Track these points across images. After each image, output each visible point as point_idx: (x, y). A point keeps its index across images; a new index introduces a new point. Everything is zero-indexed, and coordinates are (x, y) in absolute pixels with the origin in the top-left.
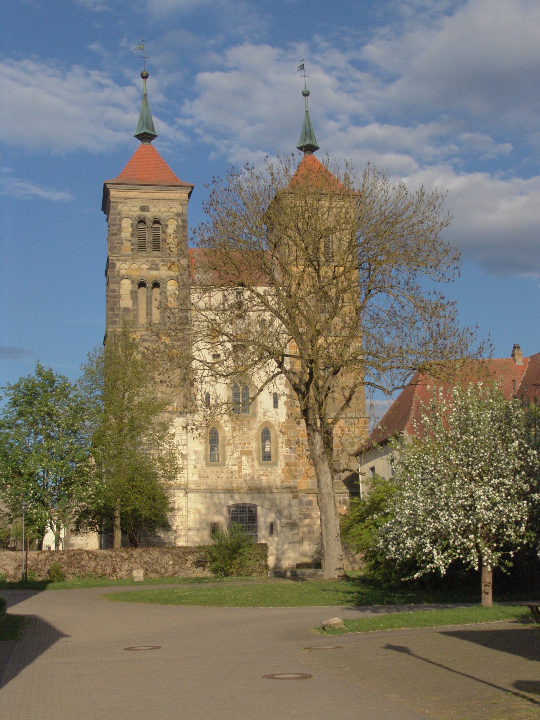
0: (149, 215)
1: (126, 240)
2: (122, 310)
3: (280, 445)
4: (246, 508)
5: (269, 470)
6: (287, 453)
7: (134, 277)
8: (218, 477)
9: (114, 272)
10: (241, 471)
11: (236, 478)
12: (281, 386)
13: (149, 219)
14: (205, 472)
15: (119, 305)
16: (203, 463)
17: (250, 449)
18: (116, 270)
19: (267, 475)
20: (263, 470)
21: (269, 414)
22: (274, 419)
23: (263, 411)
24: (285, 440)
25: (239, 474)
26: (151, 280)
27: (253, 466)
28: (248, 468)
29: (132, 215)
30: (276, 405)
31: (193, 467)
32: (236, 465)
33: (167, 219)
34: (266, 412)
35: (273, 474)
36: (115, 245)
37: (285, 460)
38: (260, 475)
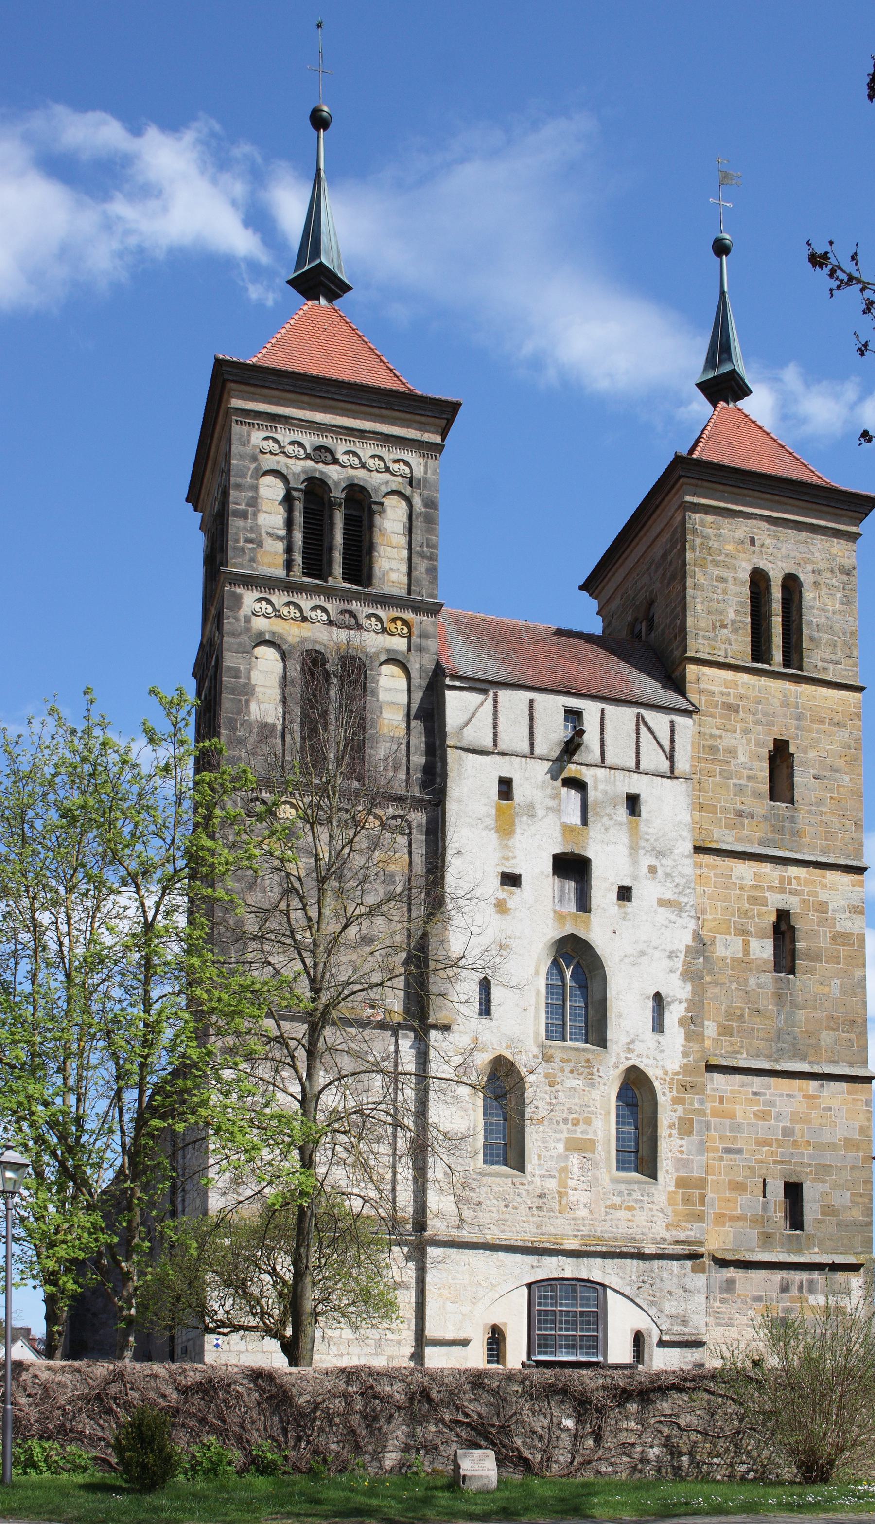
3: (663, 1131)
5: (637, 1195)
6: (682, 1152)
7: (290, 639)
8: (506, 1206)
10: (567, 1194)
11: (551, 1210)
12: (672, 975)
17: (590, 1136)
19: (630, 1209)
20: (620, 1193)
21: (639, 1047)
22: (651, 1062)
23: (624, 1039)
24: (679, 1119)
30: (658, 1026)
34: (632, 1041)
37: (677, 1170)
38: (613, 1207)
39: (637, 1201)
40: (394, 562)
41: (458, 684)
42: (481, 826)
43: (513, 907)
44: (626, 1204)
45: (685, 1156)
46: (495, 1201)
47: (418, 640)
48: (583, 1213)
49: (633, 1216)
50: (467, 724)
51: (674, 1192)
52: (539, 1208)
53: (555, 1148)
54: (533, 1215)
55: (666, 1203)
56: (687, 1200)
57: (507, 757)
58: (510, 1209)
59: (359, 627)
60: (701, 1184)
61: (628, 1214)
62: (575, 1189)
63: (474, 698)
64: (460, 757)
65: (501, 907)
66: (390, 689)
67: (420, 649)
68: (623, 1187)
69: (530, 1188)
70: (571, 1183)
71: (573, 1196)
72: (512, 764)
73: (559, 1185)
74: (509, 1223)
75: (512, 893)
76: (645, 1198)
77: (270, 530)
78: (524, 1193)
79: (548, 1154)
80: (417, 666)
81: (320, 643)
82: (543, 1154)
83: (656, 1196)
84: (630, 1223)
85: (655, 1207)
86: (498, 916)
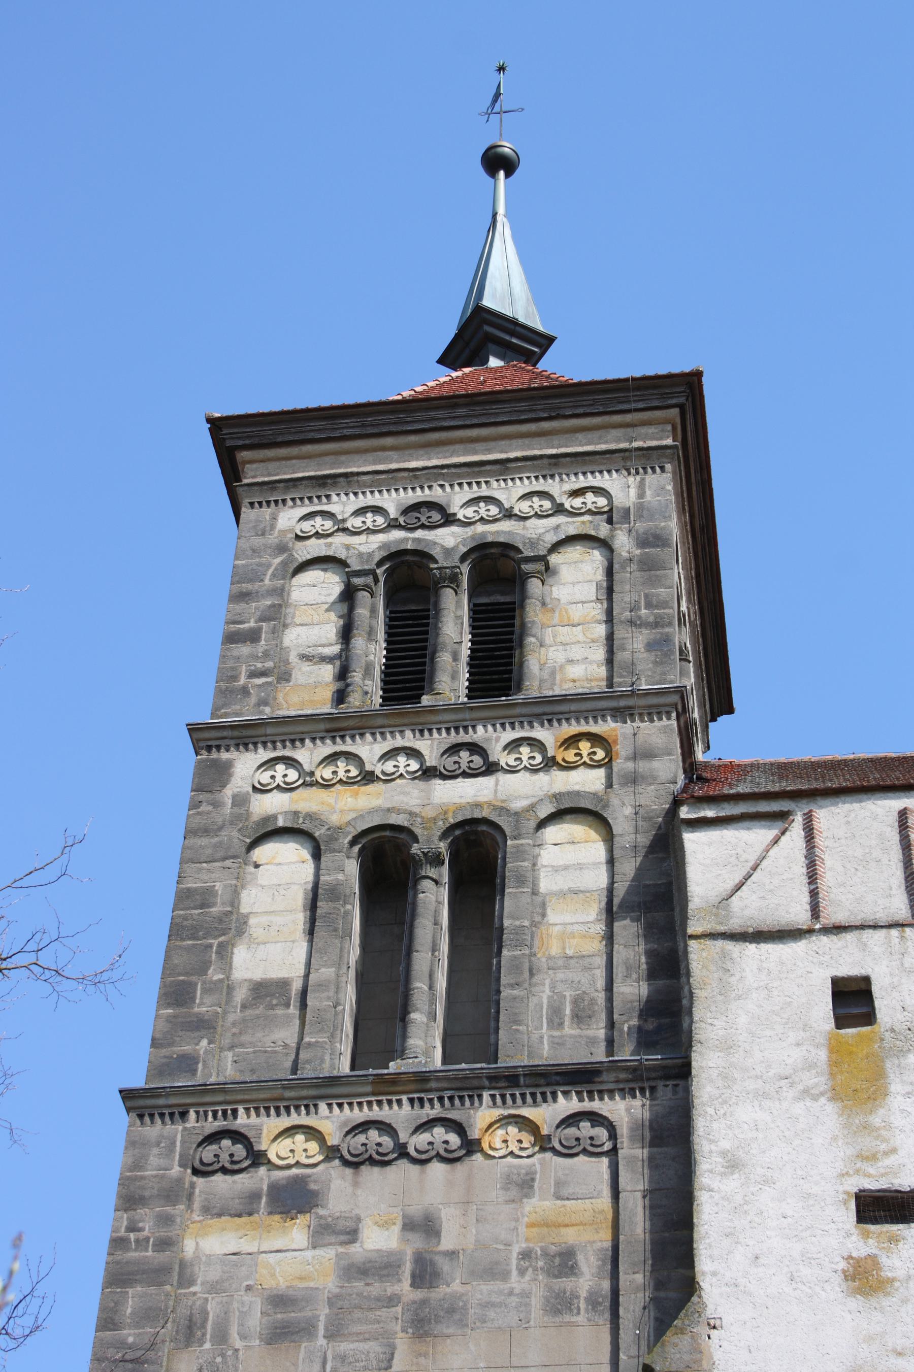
0: (447, 540)
1: (305, 657)
2: (240, 995)
7: (335, 819)
9: (216, 804)
13: (448, 552)
15: (227, 967)
18: (228, 792)
26: (442, 825)
29: (348, 547)
33: (551, 538)
36: (242, 680)
40: (576, 648)
41: (710, 813)
42: (790, 1094)
43: (900, 1273)
47: (630, 765)
50: (739, 887)
57: (849, 937)
59: (491, 768)
63: (756, 837)
64: (724, 955)
65: (863, 1278)
66: (566, 868)
67: (633, 780)
72: (864, 947)
75: (894, 1240)
77: (307, 651)
80: (628, 811)
81: (399, 811)
86: (854, 1303)
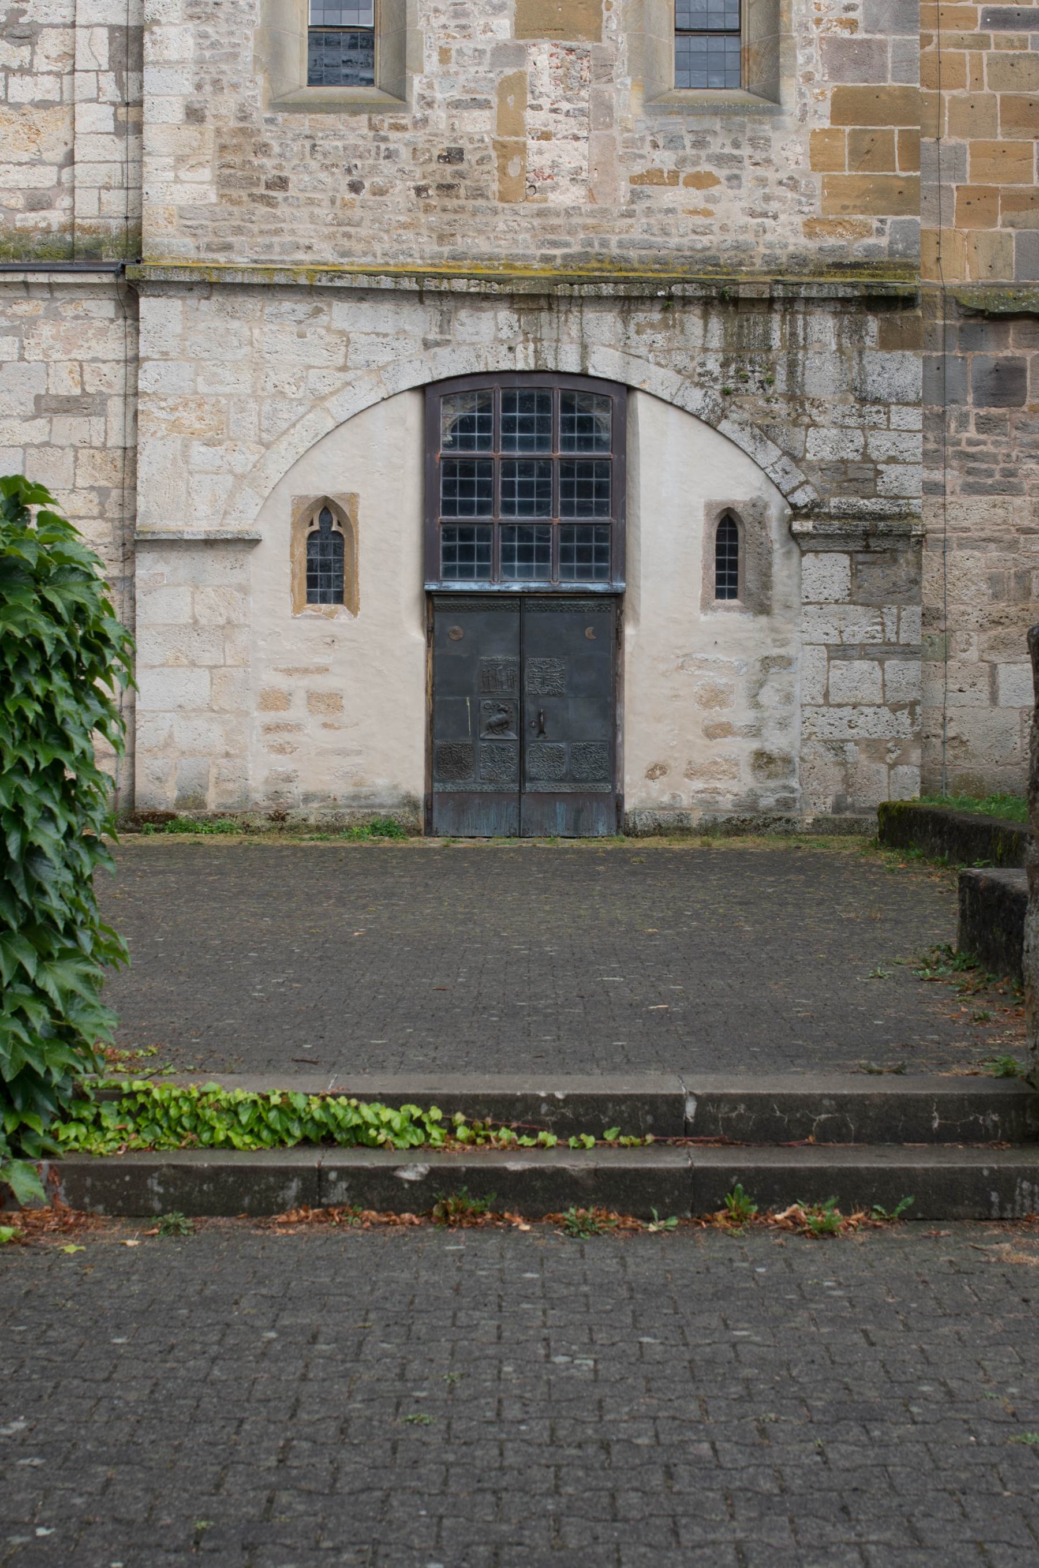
4: (544, 404)
6: (852, 25)
8: (355, 187)
10: (522, 150)
11: (479, 193)
14: (263, 149)
16: (255, 90)
19: (699, 181)
20: (673, 142)
25: (502, 170)
27: (603, 111)
28: (568, 126)
31: (180, 115)
32: (485, 105)
35: (749, 173)
37: (836, 72)
38: (653, 177)
39: (720, 160)
44: (690, 170)
45: (860, 35)
46: (323, 176)
48: (567, 196)
49: (711, 199)
51: (825, 132)
52: (447, 188)
53: (487, 29)
54: (428, 209)
55: (806, 164)
56: (864, 154)
58: (365, 194)
60: (907, 108)
61: (695, 197)
62: (546, 136)
68: (680, 125)
69: (420, 137)
70: (533, 119)
71: (539, 156)
73: (501, 126)
74: (363, 232)
76: (746, 151)
78: (405, 153)
79: (468, 46)
82: (455, 46)
83: (776, 145)
84: (700, 220)
85: (771, 175)
